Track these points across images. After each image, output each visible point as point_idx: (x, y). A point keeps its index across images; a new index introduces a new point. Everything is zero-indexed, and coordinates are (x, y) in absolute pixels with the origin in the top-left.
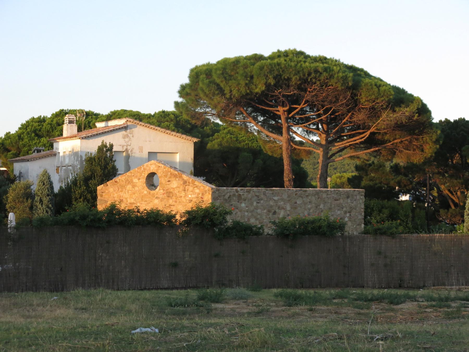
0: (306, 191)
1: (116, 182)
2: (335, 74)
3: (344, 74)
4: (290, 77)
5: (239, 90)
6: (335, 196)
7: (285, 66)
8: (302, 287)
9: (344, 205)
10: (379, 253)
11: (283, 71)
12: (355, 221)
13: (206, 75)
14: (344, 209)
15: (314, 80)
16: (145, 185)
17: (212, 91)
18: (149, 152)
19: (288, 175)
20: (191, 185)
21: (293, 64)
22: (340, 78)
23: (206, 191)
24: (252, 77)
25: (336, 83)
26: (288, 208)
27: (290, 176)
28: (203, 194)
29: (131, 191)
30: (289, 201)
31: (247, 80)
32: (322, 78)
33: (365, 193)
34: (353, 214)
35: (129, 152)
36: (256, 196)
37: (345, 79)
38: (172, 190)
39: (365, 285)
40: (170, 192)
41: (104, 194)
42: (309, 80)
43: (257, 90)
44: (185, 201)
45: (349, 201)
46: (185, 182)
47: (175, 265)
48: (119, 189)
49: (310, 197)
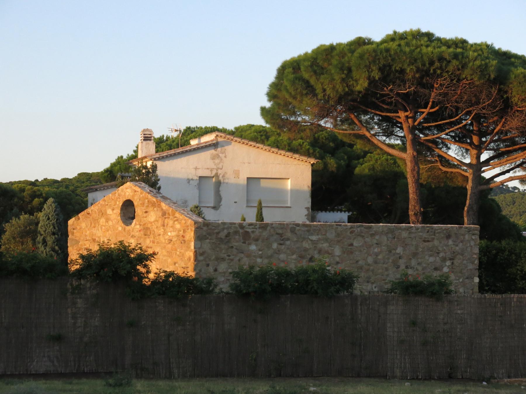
0: (370, 227)
1: (88, 214)
2: (469, 62)
3: (483, 62)
4: (403, 68)
5: (334, 88)
6: (425, 235)
7: (396, 53)
8: (280, 375)
9: (441, 249)
10: (414, 323)
11: (393, 60)
12: (461, 272)
13: (293, 69)
14: (441, 255)
15: (439, 72)
16: (119, 218)
17: (299, 90)
18: (247, 178)
19: (415, 207)
20: (171, 217)
21: (407, 49)
22: (475, 67)
23: (188, 226)
24: (350, 70)
25: (471, 75)
26: (337, 251)
27: (417, 208)
28: (184, 231)
29: (104, 226)
30: (339, 241)
31: (343, 73)
32: (451, 68)
33: (481, 231)
34: (457, 262)
35: (221, 178)
36: (277, 234)
37: (483, 69)
38: (149, 225)
39: (389, 374)
40: (148, 229)
41: (75, 231)
42: (432, 71)
43: (358, 88)
44: (164, 241)
45: (450, 242)
46: (164, 214)
47: (58, 339)
48: (91, 224)
49: (377, 237)
